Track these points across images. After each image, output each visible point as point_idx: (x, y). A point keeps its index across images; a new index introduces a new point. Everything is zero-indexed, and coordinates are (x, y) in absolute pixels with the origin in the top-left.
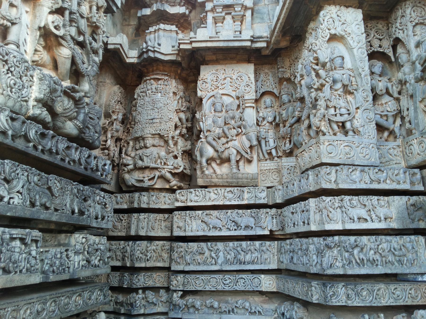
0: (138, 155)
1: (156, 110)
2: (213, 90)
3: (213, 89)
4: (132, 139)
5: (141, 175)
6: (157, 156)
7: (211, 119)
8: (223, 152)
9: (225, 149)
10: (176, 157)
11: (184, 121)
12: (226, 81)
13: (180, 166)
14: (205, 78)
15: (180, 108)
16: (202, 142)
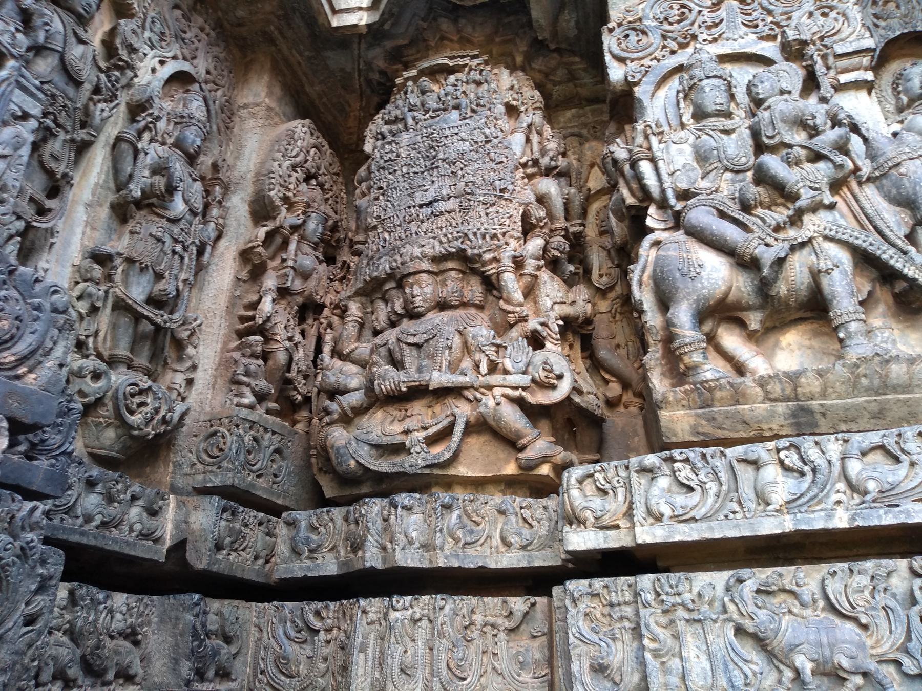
0: (383, 351)
1: (444, 168)
2: (673, 52)
3: (674, 45)
4: (358, 293)
5: (398, 428)
6: (457, 341)
7: (688, 149)
8: (780, 262)
9: (793, 249)
10: (536, 341)
11: (558, 203)
12: (722, 13)
13: (560, 377)
14: (631, 19)
15: (537, 155)
16: (657, 243)
